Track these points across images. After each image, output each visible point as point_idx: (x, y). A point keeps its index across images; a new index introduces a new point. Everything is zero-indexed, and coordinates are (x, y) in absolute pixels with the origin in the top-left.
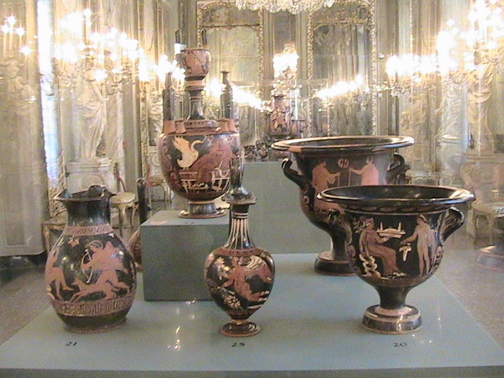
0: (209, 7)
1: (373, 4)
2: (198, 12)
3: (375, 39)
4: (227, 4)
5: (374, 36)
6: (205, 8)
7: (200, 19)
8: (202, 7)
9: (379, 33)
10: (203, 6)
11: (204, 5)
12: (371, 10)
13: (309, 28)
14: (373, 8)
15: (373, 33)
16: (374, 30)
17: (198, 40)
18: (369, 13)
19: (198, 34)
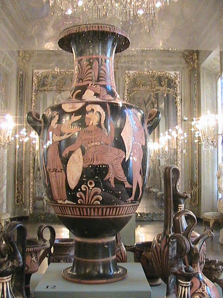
0: (43, 75)
1: (179, 76)
2: (34, 78)
3: (180, 104)
4: (58, 72)
5: (179, 103)
6: (40, 76)
7: (35, 85)
8: (37, 75)
9: (183, 100)
10: (39, 74)
11: (39, 73)
12: (177, 81)
13: (126, 94)
14: (179, 79)
15: (178, 100)
16: (179, 97)
17: (33, 101)
18: (175, 83)
19: (33, 96)
